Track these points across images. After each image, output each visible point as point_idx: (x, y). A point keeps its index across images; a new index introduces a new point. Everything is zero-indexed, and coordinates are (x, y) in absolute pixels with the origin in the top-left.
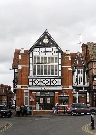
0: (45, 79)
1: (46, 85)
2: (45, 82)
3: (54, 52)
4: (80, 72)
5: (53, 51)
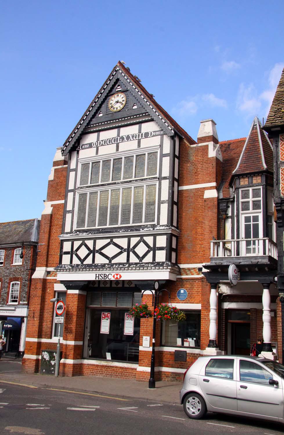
0: (109, 240)
1: (113, 261)
2: (111, 251)
3: (147, 135)
4: (251, 199)
5: (143, 131)
